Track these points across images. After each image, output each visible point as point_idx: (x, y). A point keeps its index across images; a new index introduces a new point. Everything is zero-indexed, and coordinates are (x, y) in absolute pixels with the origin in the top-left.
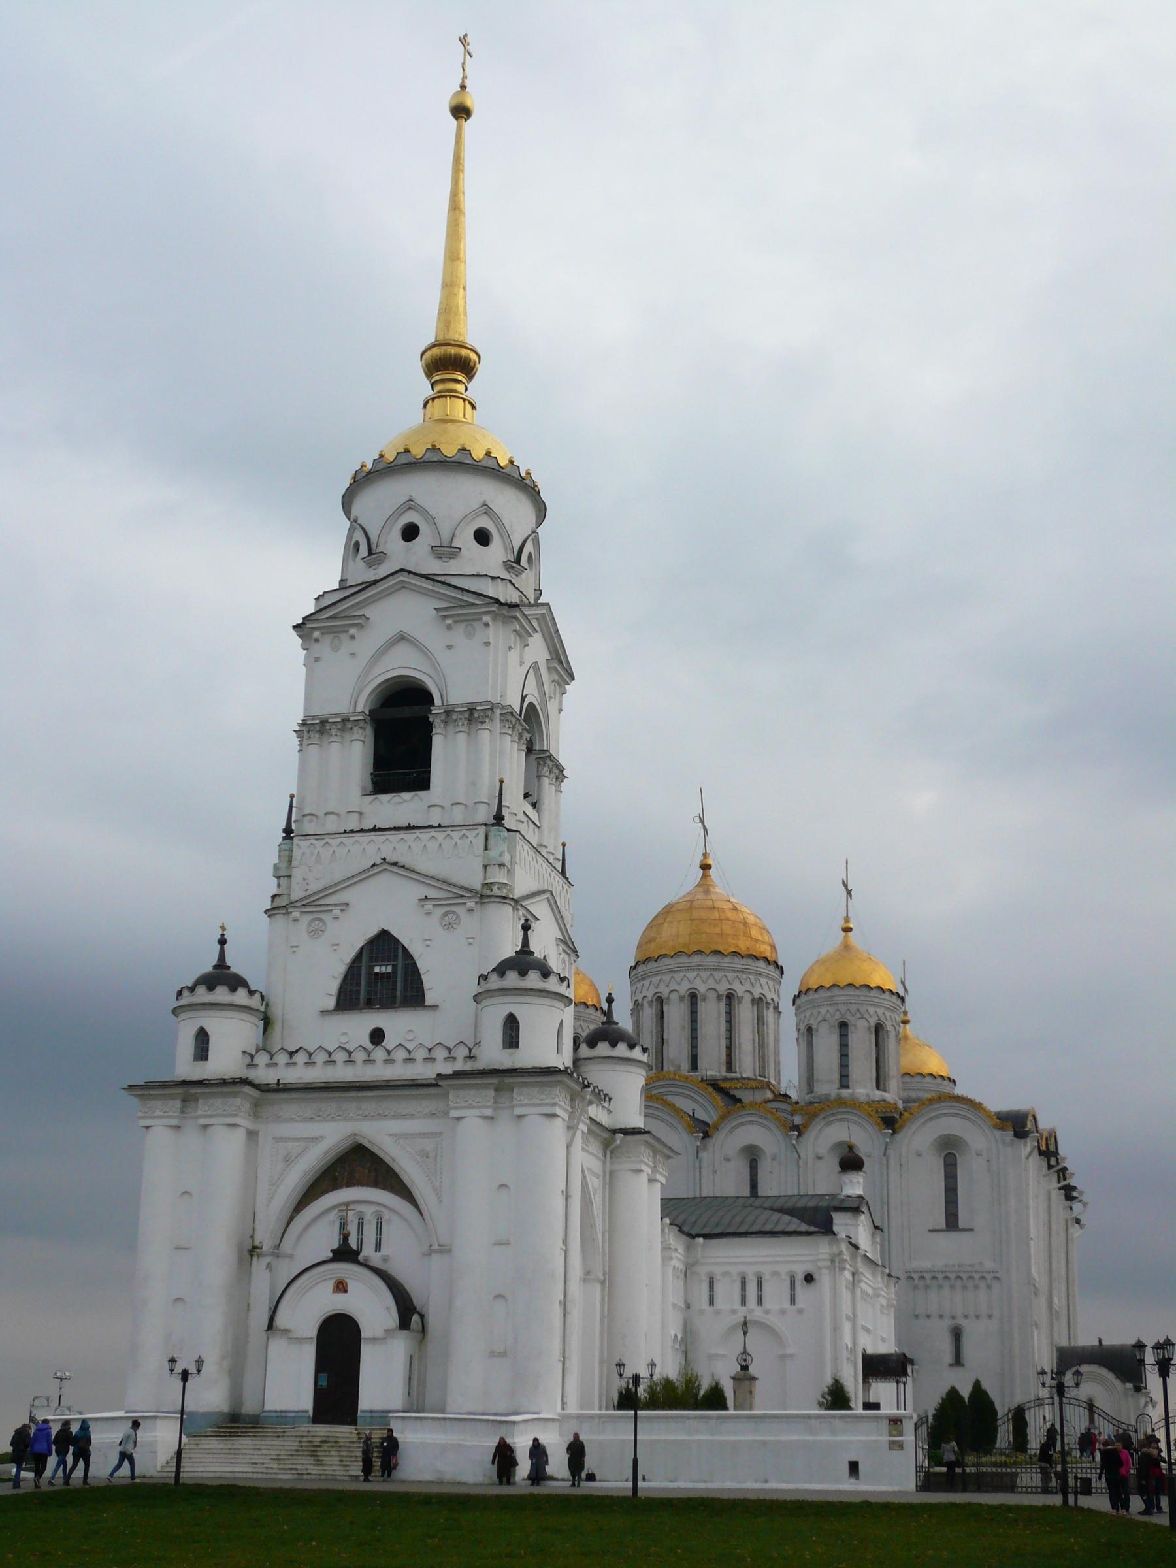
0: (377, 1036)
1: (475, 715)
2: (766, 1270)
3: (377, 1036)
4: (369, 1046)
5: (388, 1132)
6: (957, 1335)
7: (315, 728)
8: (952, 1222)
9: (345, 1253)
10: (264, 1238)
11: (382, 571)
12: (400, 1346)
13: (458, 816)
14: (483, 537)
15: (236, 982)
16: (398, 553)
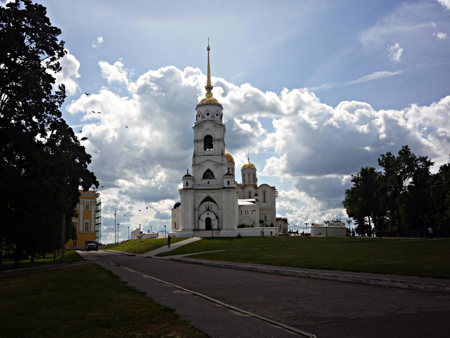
0: (209, 182)
1: (219, 140)
2: (249, 210)
3: (209, 182)
4: (207, 183)
5: (212, 195)
6: (265, 217)
7: (196, 141)
8: (264, 201)
9: (208, 210)
10: (197, 208)
11: (204, 120)
12: (216, 221)
13: (217, 154)
14: (217, 115)
15: (191, 176)
16: (207, 117)
